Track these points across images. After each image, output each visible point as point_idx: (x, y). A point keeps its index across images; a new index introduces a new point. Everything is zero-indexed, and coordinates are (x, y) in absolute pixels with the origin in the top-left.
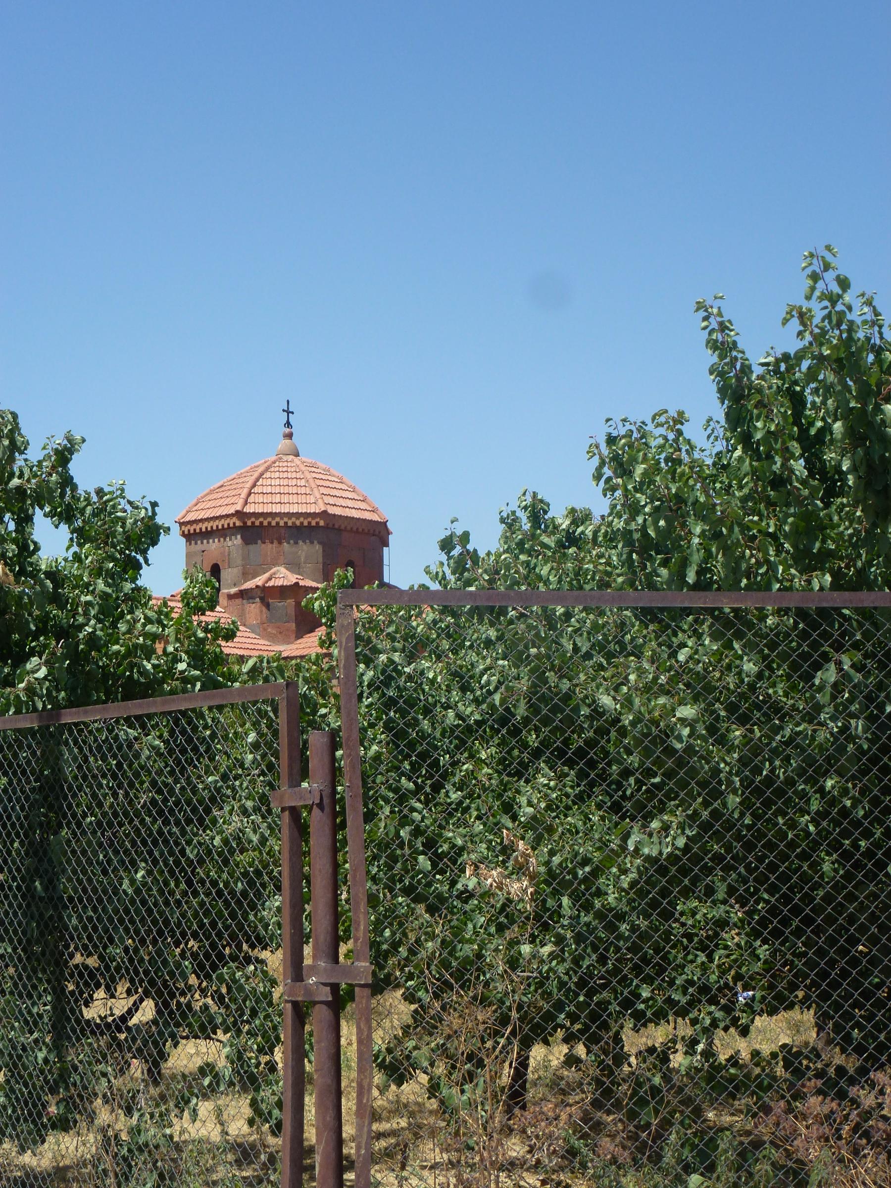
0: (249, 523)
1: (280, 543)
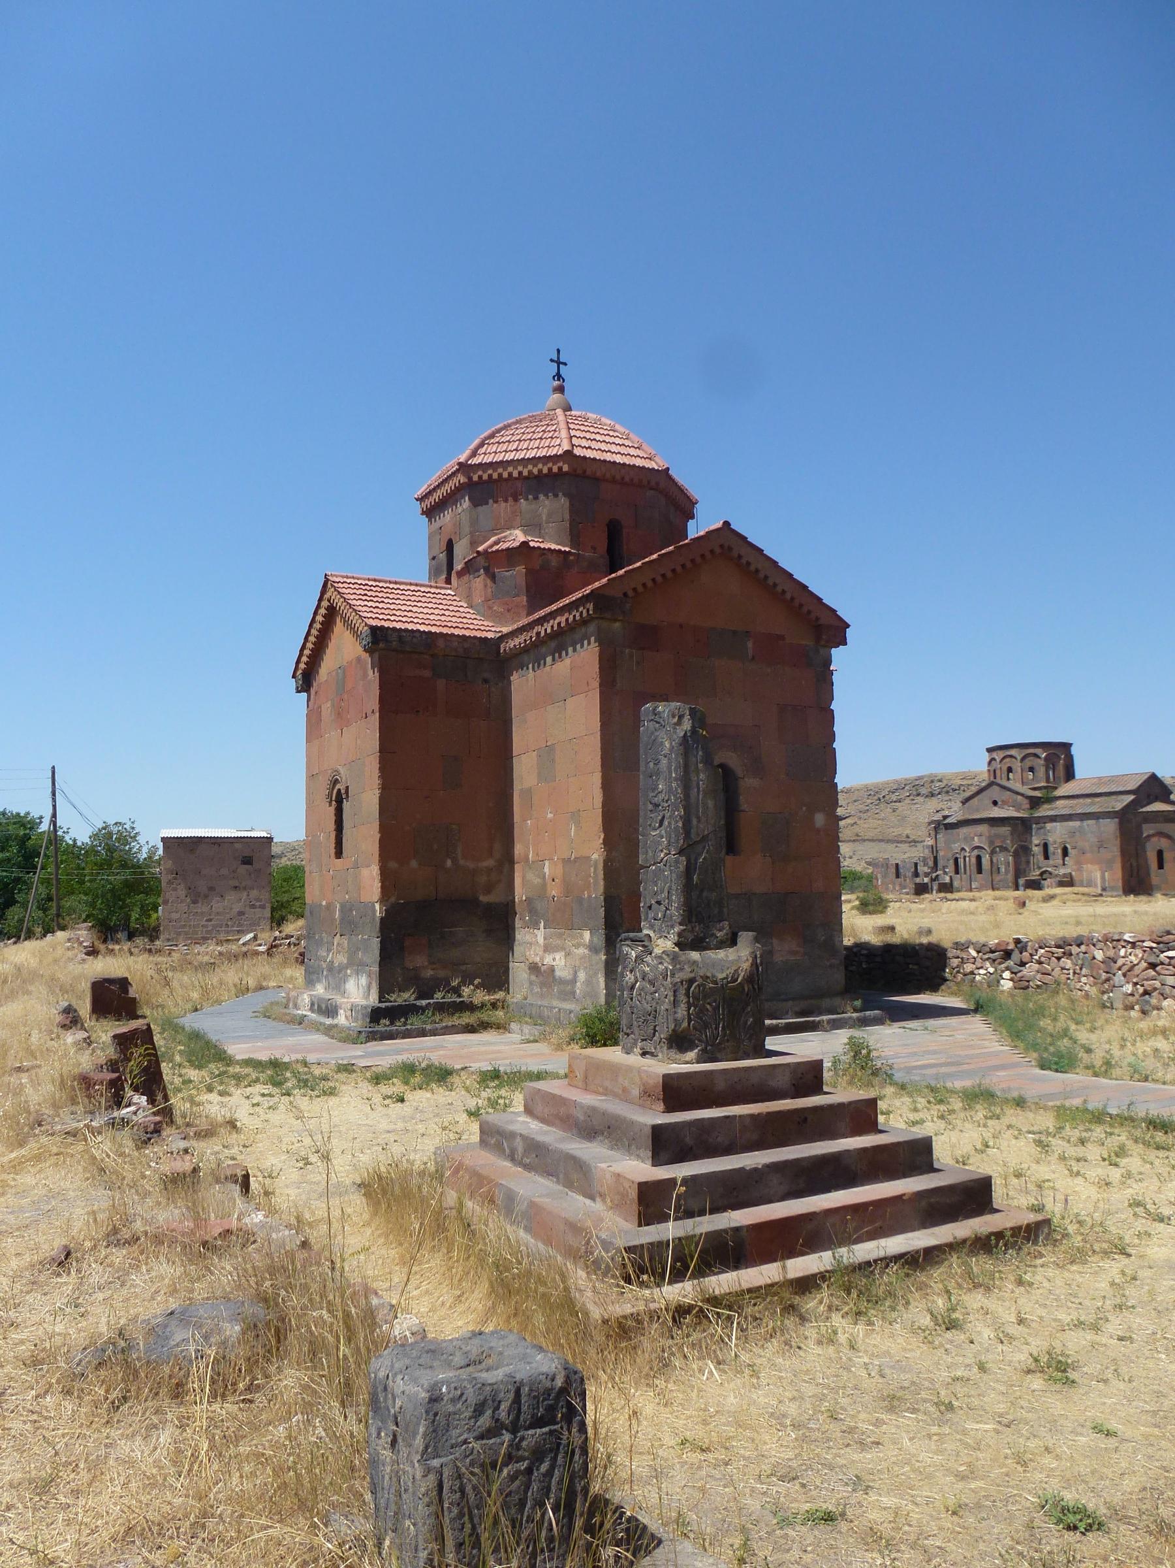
0: (475, 478)
1: (516, 500)
